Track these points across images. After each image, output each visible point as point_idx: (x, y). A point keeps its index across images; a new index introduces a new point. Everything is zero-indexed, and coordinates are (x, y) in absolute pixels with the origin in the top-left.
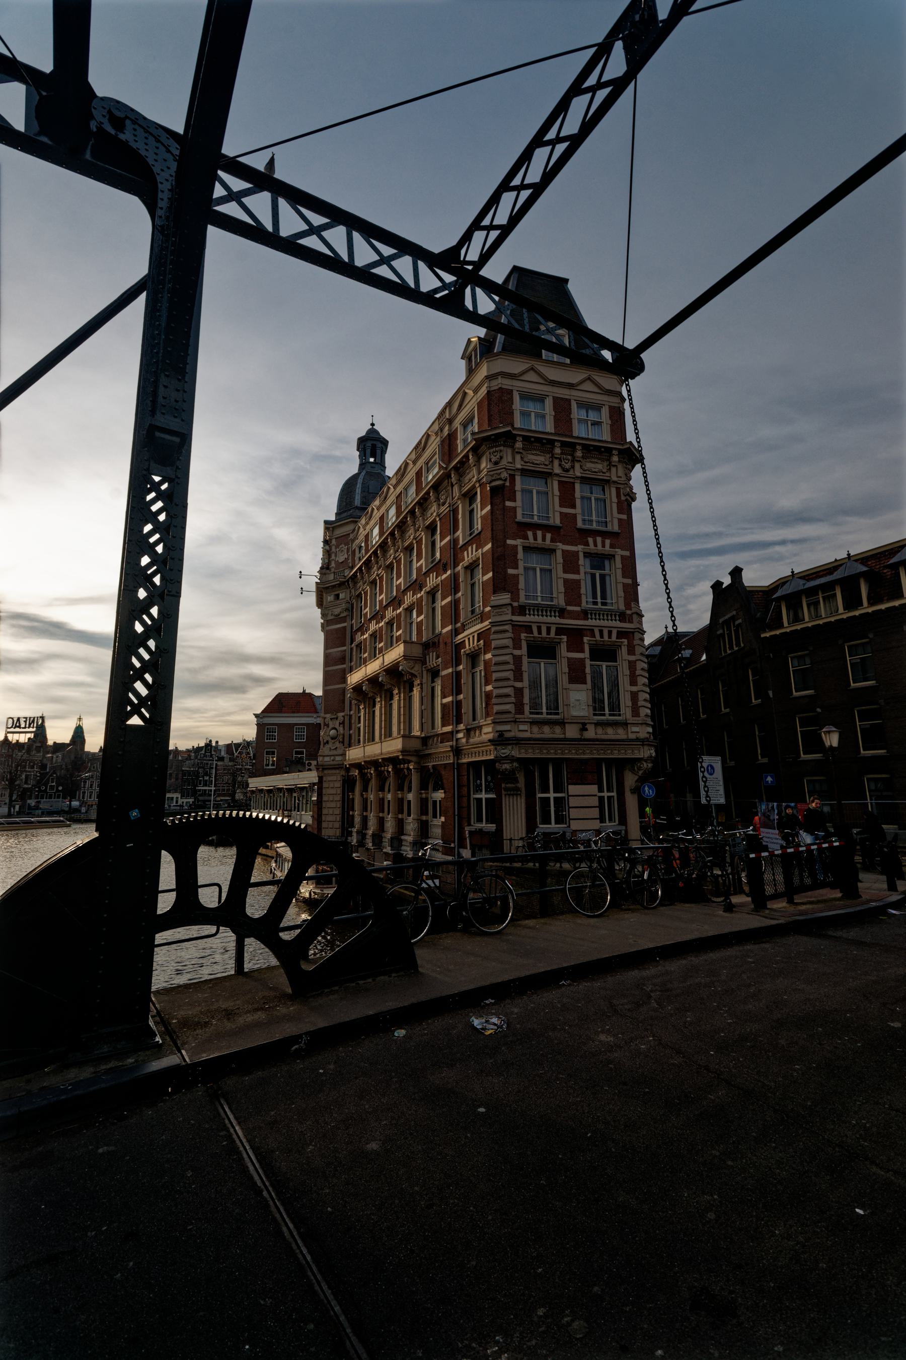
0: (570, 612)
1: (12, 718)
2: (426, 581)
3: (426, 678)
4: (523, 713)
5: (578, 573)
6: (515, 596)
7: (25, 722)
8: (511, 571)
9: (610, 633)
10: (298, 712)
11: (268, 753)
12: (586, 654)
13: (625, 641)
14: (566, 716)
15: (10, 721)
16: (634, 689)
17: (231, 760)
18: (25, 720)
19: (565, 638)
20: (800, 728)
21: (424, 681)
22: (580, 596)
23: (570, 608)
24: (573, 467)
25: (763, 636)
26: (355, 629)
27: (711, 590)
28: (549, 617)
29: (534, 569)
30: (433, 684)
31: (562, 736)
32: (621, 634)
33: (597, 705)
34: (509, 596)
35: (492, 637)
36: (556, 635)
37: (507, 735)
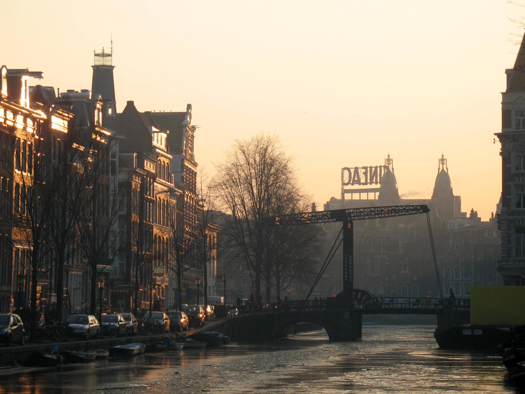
1: (348, 169)
7: (365, 173)
15: (346, 173)
18: (364, 170)
28: (522, 216)
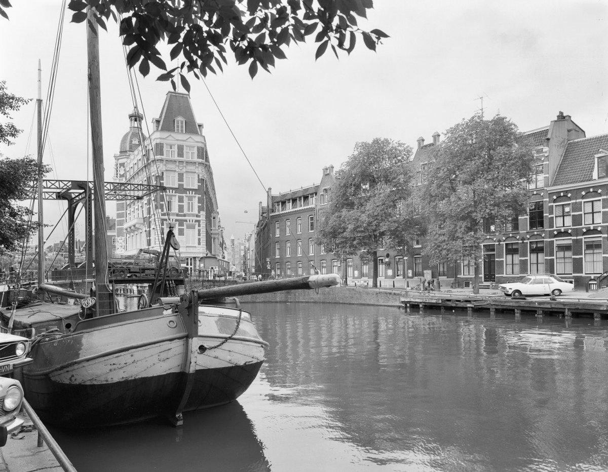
13: (197, 223)
19: (178, 222)
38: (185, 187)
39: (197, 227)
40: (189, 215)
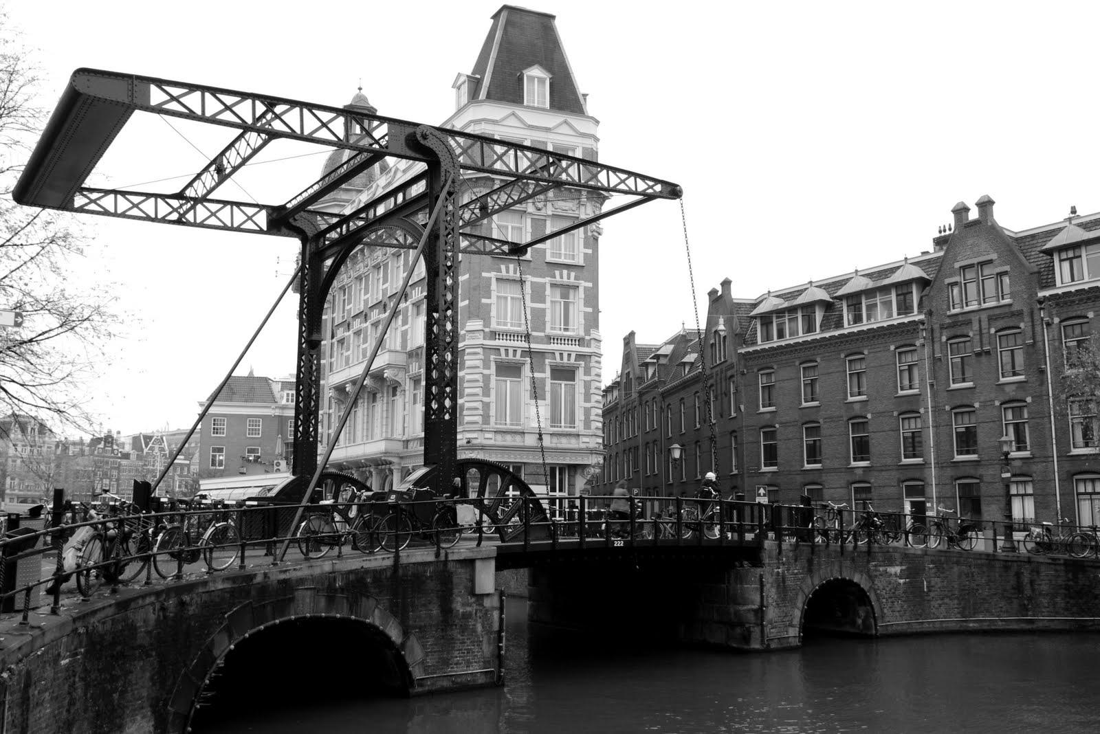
0: (537, 337)
2: (411, 293)
3: (408, 386)
4: (489, 424)
5: (544, 302)
6: (487, 322)
8: (484, 301)
9: (569, 355)
10: (252, 400)
11: (214, 450)
12: (548, 373)
14: (526, 427)
16: (588, 405)
17: (139, 457)
20: (764, 441)
21: (407, 388)
22: (544, 323)
23: (534, 334)
24: (545, 206)
25: (739, 351)
26: (336, 323)
27: (707, 297)
29: (506, 298)
30: (416, 392)
31: (522, 444)
32: (580, 357)
33: (555, 419)
34: (482, 323)
35: (466, 358)
36: (521, 357)
37: (474, 442)
38: (549, 259)
39: (580, 375)
40: (559, 339)
